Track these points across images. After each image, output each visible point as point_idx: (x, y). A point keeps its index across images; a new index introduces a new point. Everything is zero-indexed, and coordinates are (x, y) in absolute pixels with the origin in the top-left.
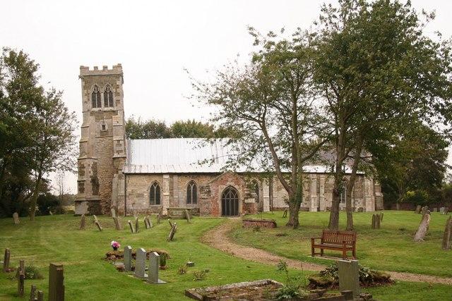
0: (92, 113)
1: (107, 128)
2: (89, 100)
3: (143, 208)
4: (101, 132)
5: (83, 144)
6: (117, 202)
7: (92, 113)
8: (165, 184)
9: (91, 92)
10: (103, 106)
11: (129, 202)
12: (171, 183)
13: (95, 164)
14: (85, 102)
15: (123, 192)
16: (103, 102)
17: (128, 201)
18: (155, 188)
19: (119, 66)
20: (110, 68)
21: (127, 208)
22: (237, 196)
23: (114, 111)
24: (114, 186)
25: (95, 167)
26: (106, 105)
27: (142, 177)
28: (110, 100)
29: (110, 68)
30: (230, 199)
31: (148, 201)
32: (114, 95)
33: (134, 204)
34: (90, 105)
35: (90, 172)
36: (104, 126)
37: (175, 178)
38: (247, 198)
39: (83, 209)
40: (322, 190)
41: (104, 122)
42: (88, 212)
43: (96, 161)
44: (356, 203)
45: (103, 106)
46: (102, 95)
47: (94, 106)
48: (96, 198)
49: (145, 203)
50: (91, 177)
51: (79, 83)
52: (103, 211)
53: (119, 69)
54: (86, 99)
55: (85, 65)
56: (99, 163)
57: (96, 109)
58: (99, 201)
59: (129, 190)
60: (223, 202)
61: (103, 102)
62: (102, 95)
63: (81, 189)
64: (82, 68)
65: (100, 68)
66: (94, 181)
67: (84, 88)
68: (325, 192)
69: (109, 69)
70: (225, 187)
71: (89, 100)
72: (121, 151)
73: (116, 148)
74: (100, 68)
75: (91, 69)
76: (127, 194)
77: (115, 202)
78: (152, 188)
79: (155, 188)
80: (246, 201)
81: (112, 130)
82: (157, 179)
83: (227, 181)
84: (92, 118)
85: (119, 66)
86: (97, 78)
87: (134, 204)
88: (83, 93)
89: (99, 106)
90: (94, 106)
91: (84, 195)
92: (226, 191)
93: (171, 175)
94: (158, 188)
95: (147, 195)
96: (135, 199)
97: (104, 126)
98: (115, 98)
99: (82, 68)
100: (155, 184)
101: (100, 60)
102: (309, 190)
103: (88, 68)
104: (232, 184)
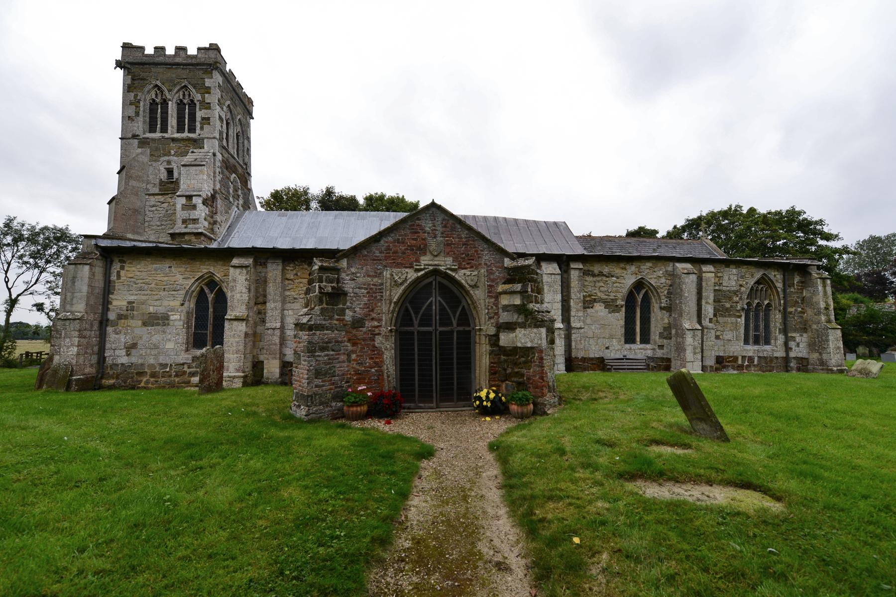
0: (144, 143)
2: (137, 114)
3: (162, 359)
7: (144, 143)
8: (238, 284)
9: (147, 96)
11: (116, 341)
16: (172, 121)
18: (211, 297)
20: (192, 51)
21: (109, 361)
22: (466, 318)
23: (194, 141)
26: (180, 129)
29: (192, 51)
30: (436, 328)
31: (182, 338)
33: (134, 346)
34: (140, 126)
37: (274, 270)
38: (510, 327)
40: (709, 310)
41: (169, 162)
44: (792, 344)
46: (172, 108)
49: (170, 345)
53: (212, 54)
54: (131, 111)
55: (135, 43)
59: (119, 302)
61: (172, 121)
62: (172, 108)
64: (126, 47)
65: (170, 51)
67: (128, 88)
68: (715, 315)
70: (412, 275)
71: (137, 114)
73: (181, 214)
74: (170, 51)
75: (149, 51)
76: (112, 316)
78: (201, 297)
79: (211, 297)
80: (505, 339)
82: (217, 271)
83: (423, 249)
84: (142, 155)
86: (160, 69)
87: (134, 346)
89: (164, 129)
90: (152, 129)
92: (415, 295)
94: (221, 300)
95: (178, 318)
98: (199, 114)
99: (126, 47)
101: (170, 32)
102: (669, 309)
104: (445, 263)
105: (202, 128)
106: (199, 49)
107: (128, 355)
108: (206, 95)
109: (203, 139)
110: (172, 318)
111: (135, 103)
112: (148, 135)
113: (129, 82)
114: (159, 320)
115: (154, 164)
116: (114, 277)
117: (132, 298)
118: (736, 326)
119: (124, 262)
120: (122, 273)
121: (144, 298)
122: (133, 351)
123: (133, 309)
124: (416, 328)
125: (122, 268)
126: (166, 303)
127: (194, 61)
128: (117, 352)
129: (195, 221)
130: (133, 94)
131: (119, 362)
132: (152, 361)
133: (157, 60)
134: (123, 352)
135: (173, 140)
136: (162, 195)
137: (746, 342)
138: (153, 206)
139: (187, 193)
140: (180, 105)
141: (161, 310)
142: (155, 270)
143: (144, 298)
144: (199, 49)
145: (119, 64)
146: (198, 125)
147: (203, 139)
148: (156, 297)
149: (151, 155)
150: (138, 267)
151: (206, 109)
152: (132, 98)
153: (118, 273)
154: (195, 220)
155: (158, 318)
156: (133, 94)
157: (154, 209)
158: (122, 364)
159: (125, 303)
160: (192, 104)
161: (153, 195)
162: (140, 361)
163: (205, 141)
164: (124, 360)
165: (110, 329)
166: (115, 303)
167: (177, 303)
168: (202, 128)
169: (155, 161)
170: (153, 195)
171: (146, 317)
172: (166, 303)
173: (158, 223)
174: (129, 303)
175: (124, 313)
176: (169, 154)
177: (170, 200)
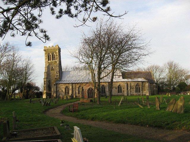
12: (72, 87)
26: (53, 60)
36: (52, 67)
43: (50, 79)
44: (143, 93)
47: (49, 60)
48: (50, 92)
51: (44, 52)
57: (50, 61)
60: (88, 93)
65: (51, 47)
67: (45, 54)
74: (51, 47)
76: (57, 91)
82: (67, 85)
88: (45, 56)
90: (49, 60)
92: (89, 89)
93: (72, 84)
94: (68, 89)
100: (67, 87)
111: (46, 56)
118: (134, 90)
124: (89, 92)
129: (58, 76)
137: (136, 92)
140: (53, 55)
160: (54, 55)
167: (64, 89)
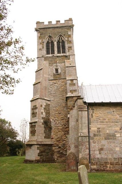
1: (59, 71)
2: (43, 47)
3: (115, 156)
4: (54, 75)
5: (36, 85)
6: (77, 147)
7: (46, 59)
9: (45, 41)
10: (56, 52)
11: (95, 146)
13: (48, 105)
14: (40, 49)
15: (85, 131)
17: (92, 145)
19: (71, 20)
20: (62, 22)
21: (92, 157)
23: (66, 56)
24: (72, 123)
25: (47, 109)
26: (59, 52)
27: (112, 109)
28: (62, 47)
32: (66, 43)
34: (44, 52)
35: (42, 113)
36: (57, 70)
39: (32, 154)
41: (57, 66)
42: (39, 158)
43: (49, 103)
45: (56, 52)
46: (55, 43)
47: (48, 53)
48: (48, 142)
50: (43, 118)
51: (35, 34)
52: (55, 157)
53: (70, 22)
54: (41, 47)
56: (52, 105)
58: (51, 145)
59: (94, 128)
62: (55, 43)
63: (33, 132)
64: (38, 23)
66: (47, 123)
67: (39, 38)
69: (61, 22)
71: (43, 47)
72: (75, 91)
73: (69, 88)
74: (54, 22)
75: (46, 23)
76: (91, 135)
77: (73, 146)
81: (65, 73)
84: (46, 63)
85: (71, 20)
86: (51, 30)
87: (101, 149)
88: (38, 42)
89: (53, 52)
91: (35, 138)
96: (104, 142)
97: (57, 70)
98: (67, 46)
99: (38, 23)
101: (53, 16)
103: (44, 23)
105: (69, 51)
106: (65, 21)
107: (100, 154)
108: (69, 38)
109: (70, 55)
110: (117, 135)
112: (47, 56)
113: (40, 35)
114: (110, 137)
115: (51, 67)
116: (90, 117)
117: (99, 126)
119: (94, 110)
120: (94, 115)
121: (104, 126)
122: (102, 151)
123: (99, 132)
125: (93, 112)
126: (113, 128)
127: (64, 25)
128: (95, 152)
130: (41, 40)
131: (97, 157)
132: (110, 157)
133: (50, 26)
134: (98, 152)
135: (58, 56)
136: (55, 80)
138: (52, 85)
139: (71, 79)
140: (58, 42)
141: (112, 132)
142: (108, 113)
143: (104, 126)
144: (65, 21)
145: (36, 30)
146: (67, 50)
147: (70, 55)
148: (109, 126)
149: (49, 63)
150: (100, 112)
151: (69, 43)
152: (41, 42)
153: (92, 114)
154: (75, 90)
155: (110, 136)
156: (41, 40)
157: (52, 86)
158: (98, 158)
159: (96, 129)
160: (63, 42)
161: (51, 80)
162: (106, 157)
163: (71, 56)
164: (98, 156)
165: (91, 141)
166: (92, 129)
168: (69, 51)
169: (51, 66)
170: (51, 80)
171: (106, 135)
172: (113, 128)
173: (54, 93)
174: (98, 128)
175: (96, 133)
176: (56, 63)
177: (58, 82)
